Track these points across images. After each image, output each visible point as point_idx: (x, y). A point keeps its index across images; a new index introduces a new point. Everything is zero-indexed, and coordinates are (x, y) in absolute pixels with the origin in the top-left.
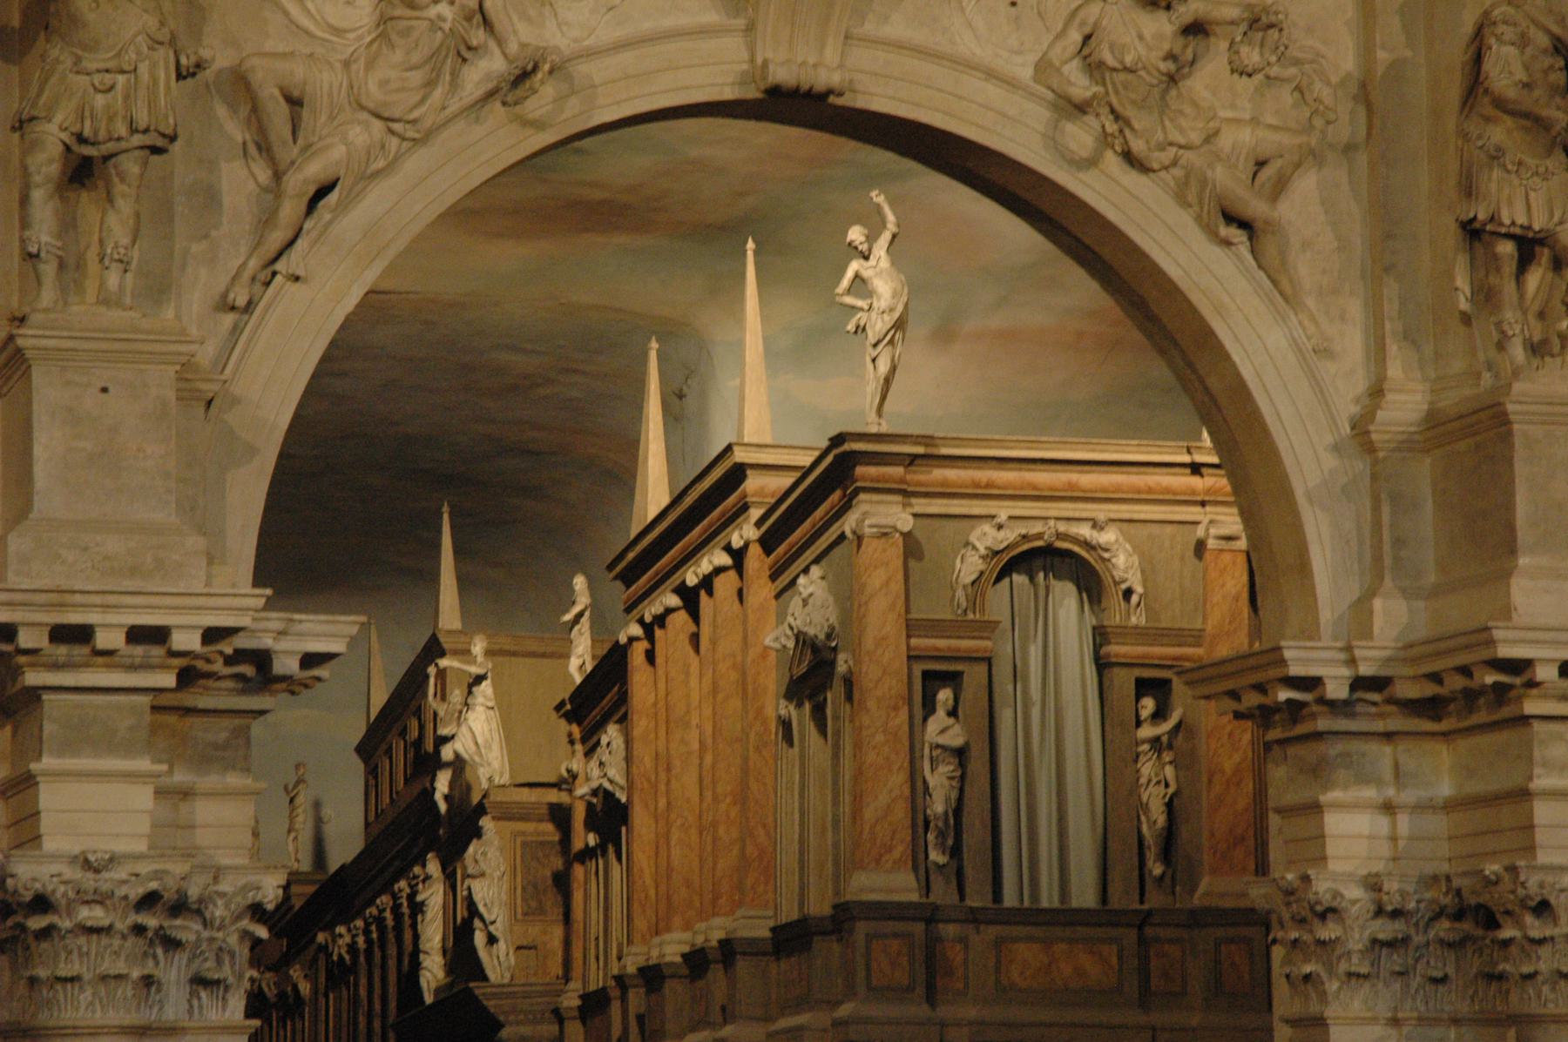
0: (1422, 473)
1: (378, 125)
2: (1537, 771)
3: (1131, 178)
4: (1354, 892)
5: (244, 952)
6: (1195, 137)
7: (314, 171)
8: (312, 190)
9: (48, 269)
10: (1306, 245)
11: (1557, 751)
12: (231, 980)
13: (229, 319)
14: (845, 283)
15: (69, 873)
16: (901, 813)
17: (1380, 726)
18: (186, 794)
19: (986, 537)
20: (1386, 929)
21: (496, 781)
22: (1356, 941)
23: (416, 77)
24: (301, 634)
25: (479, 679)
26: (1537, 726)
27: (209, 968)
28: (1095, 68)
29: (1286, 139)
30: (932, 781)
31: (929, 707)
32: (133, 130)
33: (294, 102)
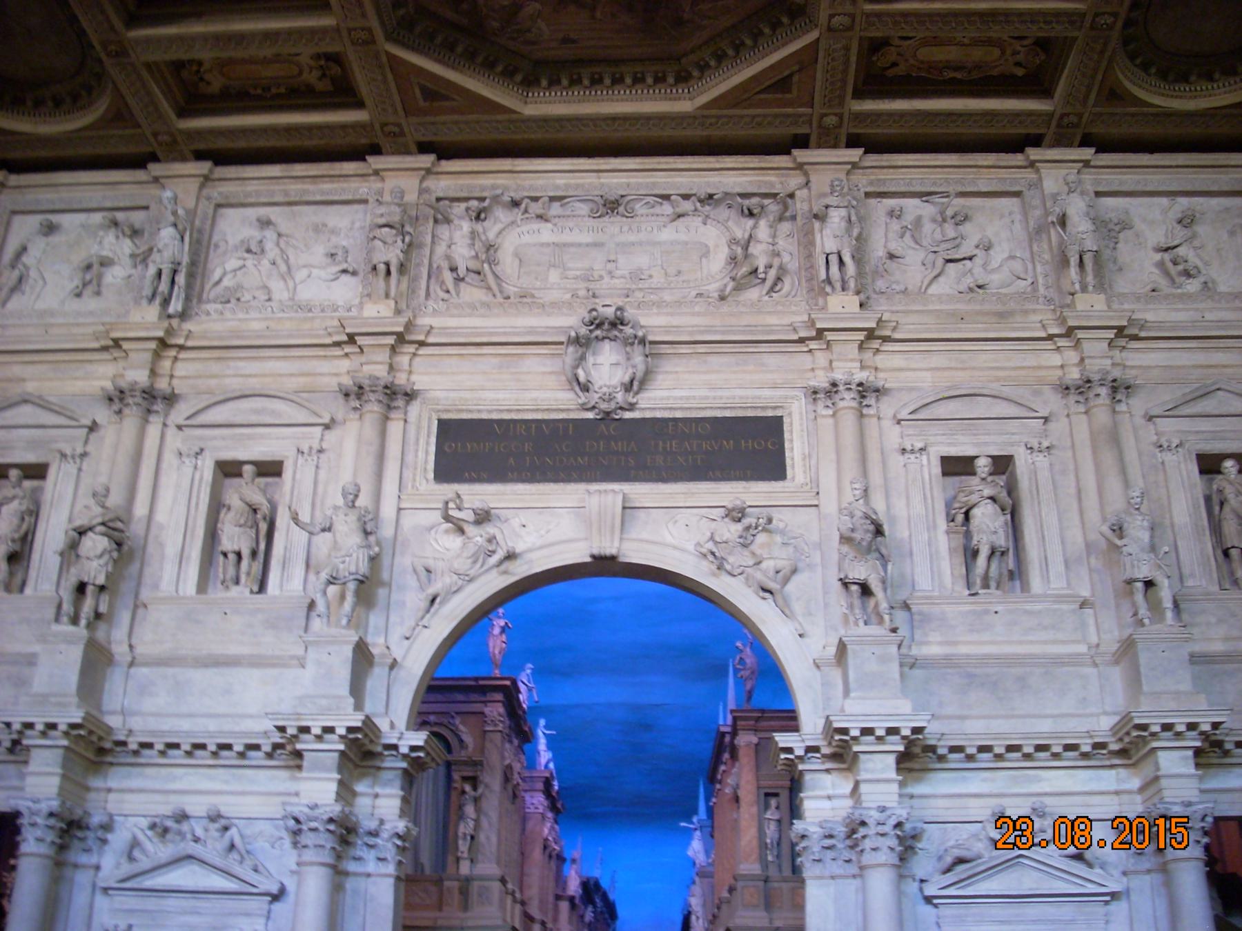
1: (455, 577)
2: (862, 773)
3: (728, 579)
4: (817, 829)
5: (394, 850)
6: (751, 563)
7: (431, 591)
8: (431, 598)
9: (325, 620)
11: (870, 765)
12: (389, 858)
13: (406, 642)
14: (737, 661)
15: (306, 810)
16: (755, 843)
17: (823, 767)
18: (376, 796)
20: (828, 842)
21: (703, 864)
22: (816, 849)
23: (470, 561)
24: (408, 739)
25: (696, 829)
26: (862, 756)
27: (382, 856)
28: (716, 543)
30: (767, 831)
31: (767, 807)
32: (350, 574)
33: (428, 571)
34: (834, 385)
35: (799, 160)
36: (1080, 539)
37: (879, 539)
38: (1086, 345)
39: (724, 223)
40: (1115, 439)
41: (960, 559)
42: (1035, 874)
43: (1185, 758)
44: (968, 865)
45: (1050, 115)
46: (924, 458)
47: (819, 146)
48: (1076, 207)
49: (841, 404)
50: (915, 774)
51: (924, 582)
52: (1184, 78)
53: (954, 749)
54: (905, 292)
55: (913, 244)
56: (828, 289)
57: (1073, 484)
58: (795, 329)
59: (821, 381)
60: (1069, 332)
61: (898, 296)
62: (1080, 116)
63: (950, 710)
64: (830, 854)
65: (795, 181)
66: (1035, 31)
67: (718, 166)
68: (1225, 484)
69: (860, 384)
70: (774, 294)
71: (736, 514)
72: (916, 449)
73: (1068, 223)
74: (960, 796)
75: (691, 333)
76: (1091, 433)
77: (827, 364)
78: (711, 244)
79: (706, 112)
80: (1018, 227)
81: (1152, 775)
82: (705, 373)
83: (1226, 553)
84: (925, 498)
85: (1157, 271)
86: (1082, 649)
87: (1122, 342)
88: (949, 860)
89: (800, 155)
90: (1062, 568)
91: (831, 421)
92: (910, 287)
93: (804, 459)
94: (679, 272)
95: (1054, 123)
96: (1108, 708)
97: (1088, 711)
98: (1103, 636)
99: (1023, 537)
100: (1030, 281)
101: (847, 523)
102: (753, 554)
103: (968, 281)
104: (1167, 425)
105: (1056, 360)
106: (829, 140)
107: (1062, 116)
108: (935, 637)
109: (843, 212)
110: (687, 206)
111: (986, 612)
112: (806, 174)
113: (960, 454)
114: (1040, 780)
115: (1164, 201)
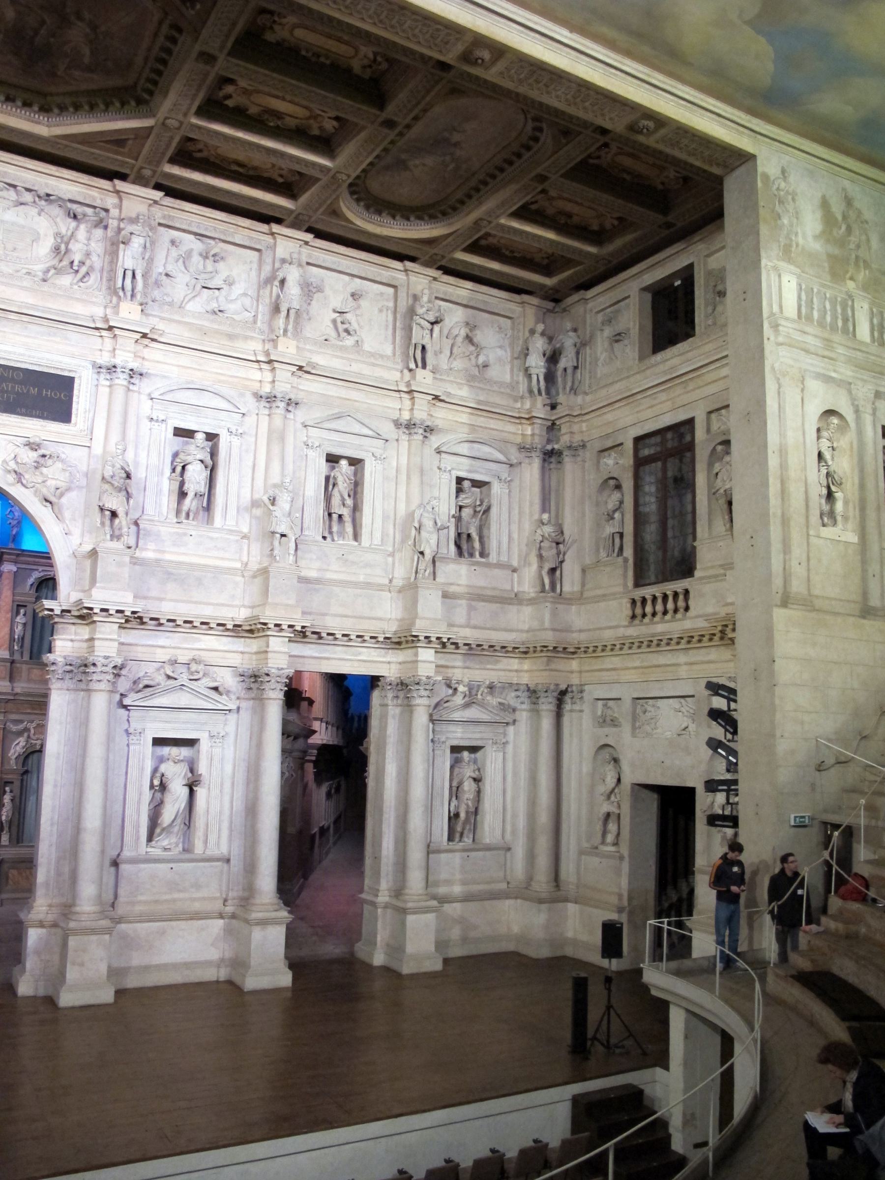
0: (88, 563)
3: (23, 489)
6: (40, 481)
10: (68, 509)
11: (103, 629)
16: (7, 637)
17: (71, 621)
19: (36, 575)
20: (69, 668)
28: (17, 463)
29: (63, 484)
31: (18, 613)
34: (115, 367)
35: (118, 188)
36: (248, 496)
37: (128, 481)
38: (278, 372)
39: (53, 219)
40: (282, 439)
41: (175, 497)
42: (188, 695)
43: (283, 642)
44: (151, 689)
45: (291, 212)
46: (164, 425)
47: (134, 183)
48: (293, 275)
49: (117, 381)
50: (126, 630)
51: (150, 510)
52: (379, 212)
53: (152, 619)
54: (171, 304)
55: (183, 269)
56: (121, 293)
57: (252, 459)
58: (94, 321)
59: (105, 359)
60: (270, 362)
61: (166, 307)
62: (310, 217)
63: (154, 593)
64: (68, 676)
65: (110, 201)
66: (297, 168)
67: (57, 174)
68: (338, 474)
69: (132, 370)
70: (81, 284)
71: (33, 446)
72: (160, 419)
73: (286, 284)
74: (153, 646)
75: (19, 307)
76: (269, 430)
77: (111, 349)
78: (42, 232)
79: (60, 141)
80: (254, 274)
81: (265, 649)
82: (26, 336)
83: (330, 515)
84: (160, 453)
85: (332, 326)
86: (238, 565)
87: (300, 373)
88: (141, 686)
89: (119, 184)
90: (235, 512)
91: (107, 390)
92: (175, 300)
93: (85, 412)
94: (15, 249)
95: (294, 215)
96: (246, 603)
97: (234, 603)
98: (251, 559)
99: (215, 488)
100: (253, 314)
101: (108, 473)
102: (42, 473)
103: (214, 305)
104: (313, 432)
105: (257, 375)
106: (141, 181)
107: (299, 214)
108: (151, 546)
109: (141, 240)
110: (28, 197)
111: (185, 534)
112: (121, 199)
113: (187, 428)
114: (199, 640)
115: (347, 278)
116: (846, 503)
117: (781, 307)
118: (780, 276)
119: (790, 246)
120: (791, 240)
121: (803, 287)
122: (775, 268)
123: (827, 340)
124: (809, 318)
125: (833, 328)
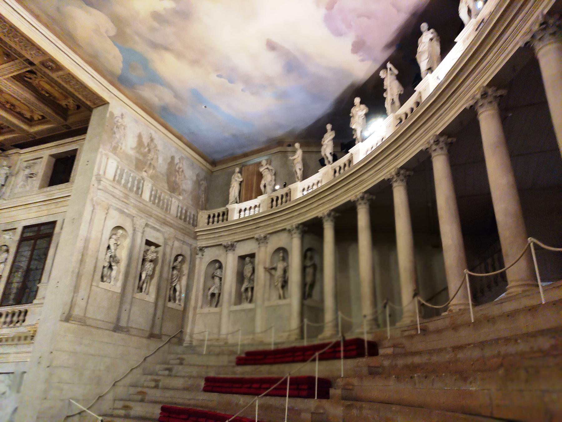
116: (118, 272)
117: (105, 173)
118: (108, 159)
119: (117, 147)
120: (118, 145)
121: (120, 167)
122: (106, 155)
123: (126, 194)
124: (119, 182)
125: (131, 190)
